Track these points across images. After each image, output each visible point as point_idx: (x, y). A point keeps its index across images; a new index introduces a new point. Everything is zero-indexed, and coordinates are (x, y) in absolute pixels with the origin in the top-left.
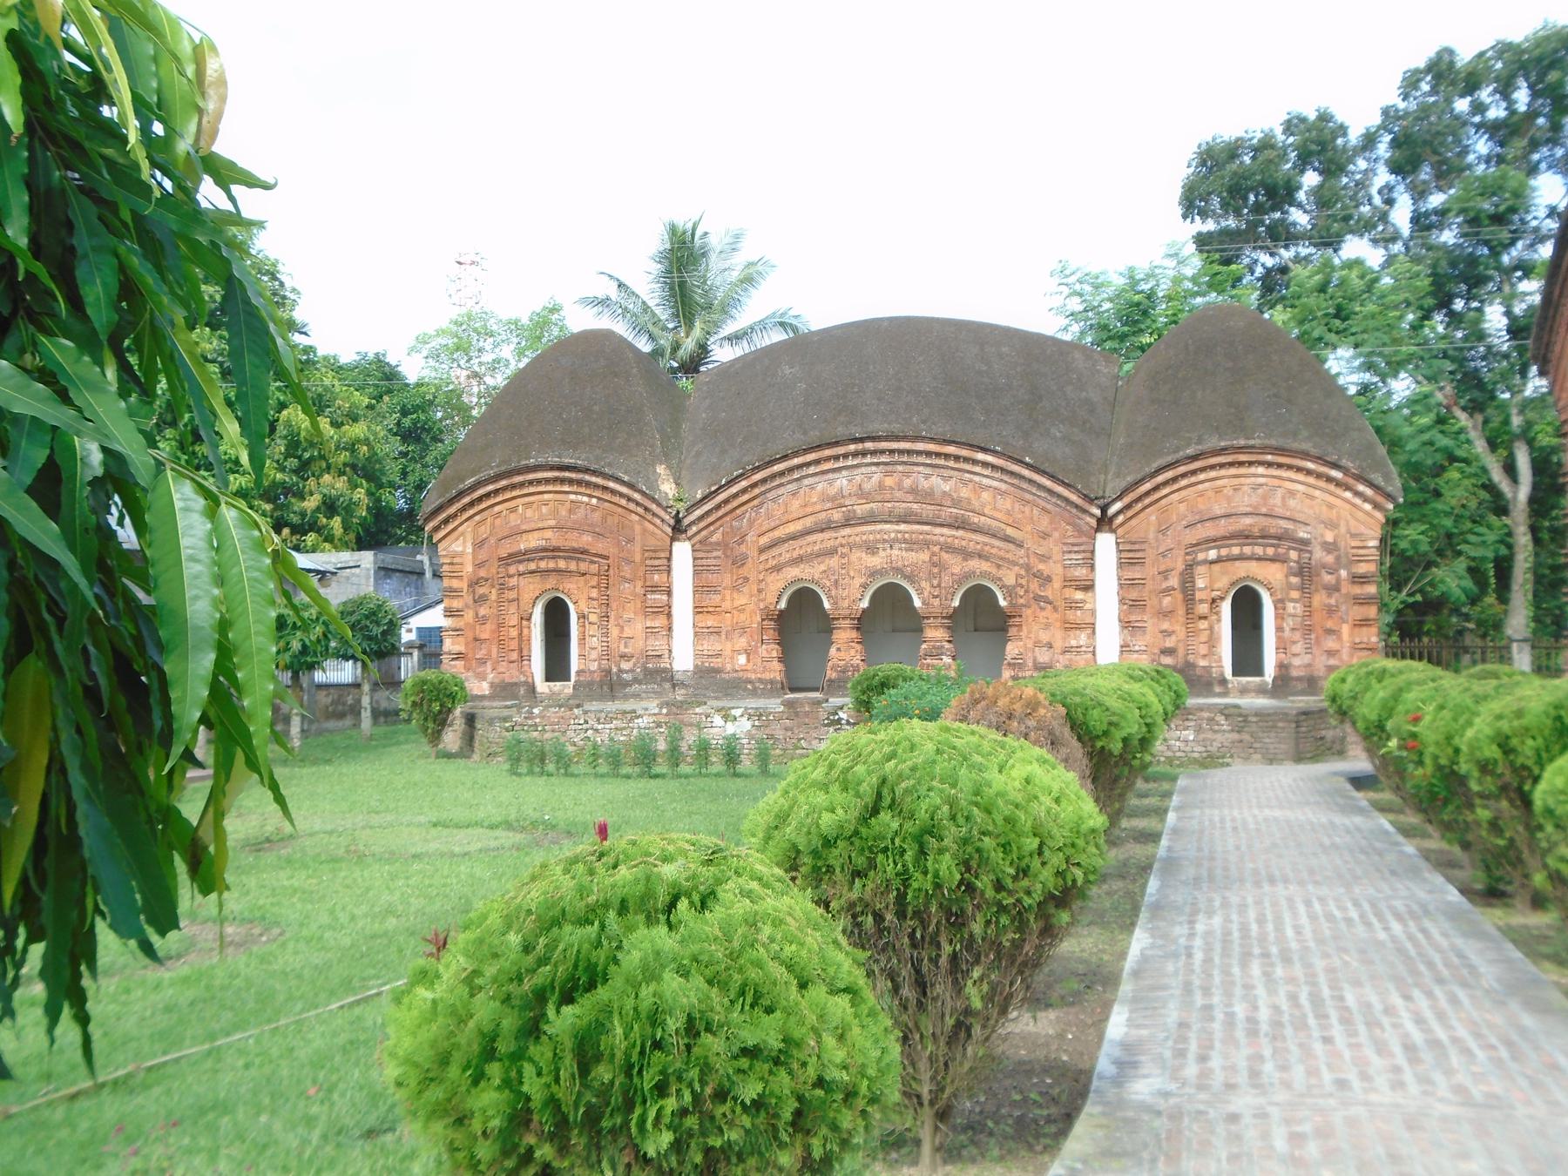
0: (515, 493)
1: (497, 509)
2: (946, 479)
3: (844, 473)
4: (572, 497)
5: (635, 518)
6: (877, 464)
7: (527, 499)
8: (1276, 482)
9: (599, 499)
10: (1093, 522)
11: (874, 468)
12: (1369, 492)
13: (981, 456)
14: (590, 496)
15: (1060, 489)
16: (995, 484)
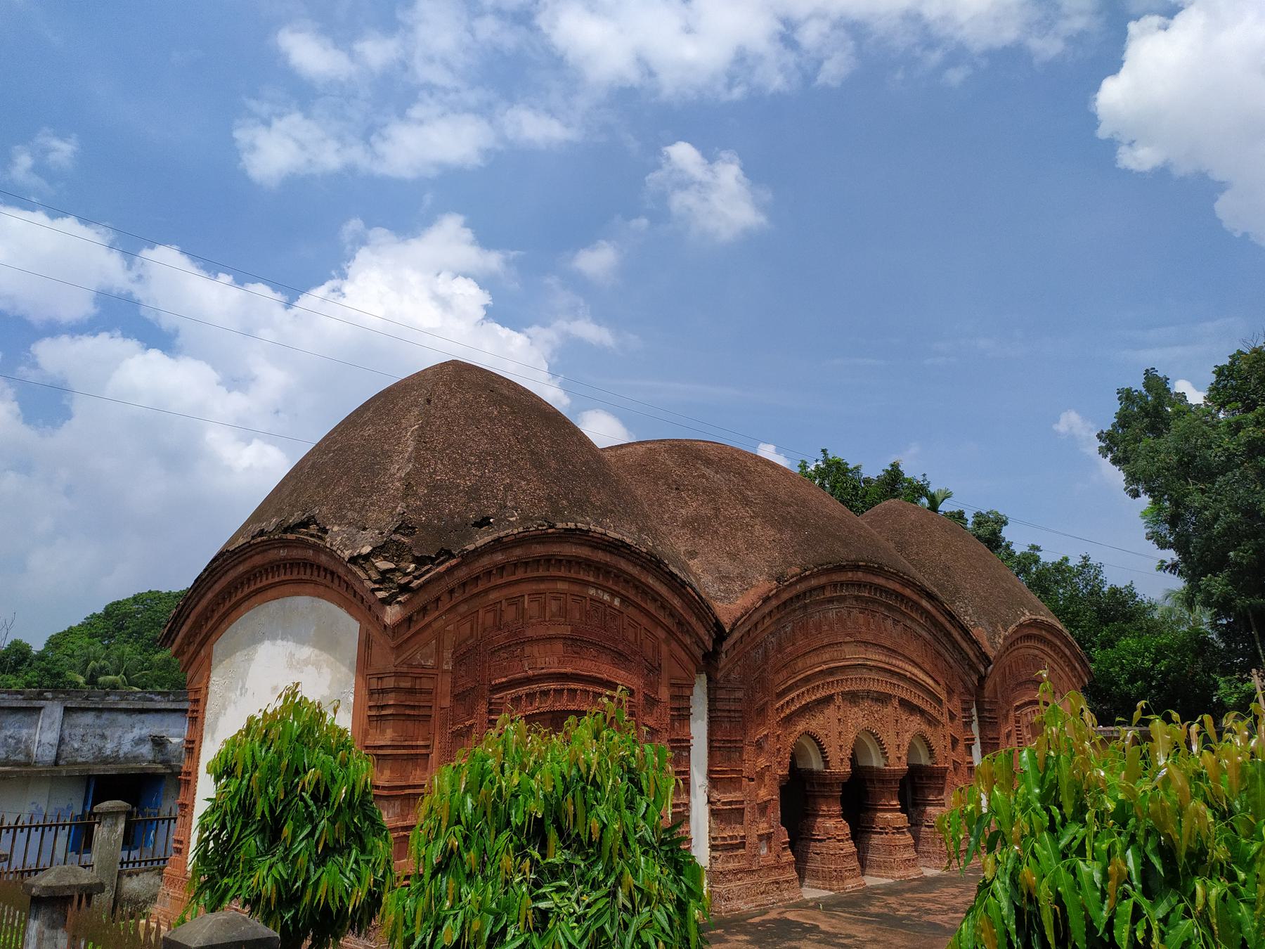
0: (520, 574)
1: (493, 596)
2: (896, 622)
3: (836, 605)
4: (592, 592)
5: (661, 634)
6: (857, 598)
7: (534, 587)
8: (1042, 655)
9: (624, 600)
10: (975, 678)
11: (854, 603)
12: (1079, 669)
13: (924, 603)
14: (614, 594)
15: (964, 645)
16: (924, 633)
